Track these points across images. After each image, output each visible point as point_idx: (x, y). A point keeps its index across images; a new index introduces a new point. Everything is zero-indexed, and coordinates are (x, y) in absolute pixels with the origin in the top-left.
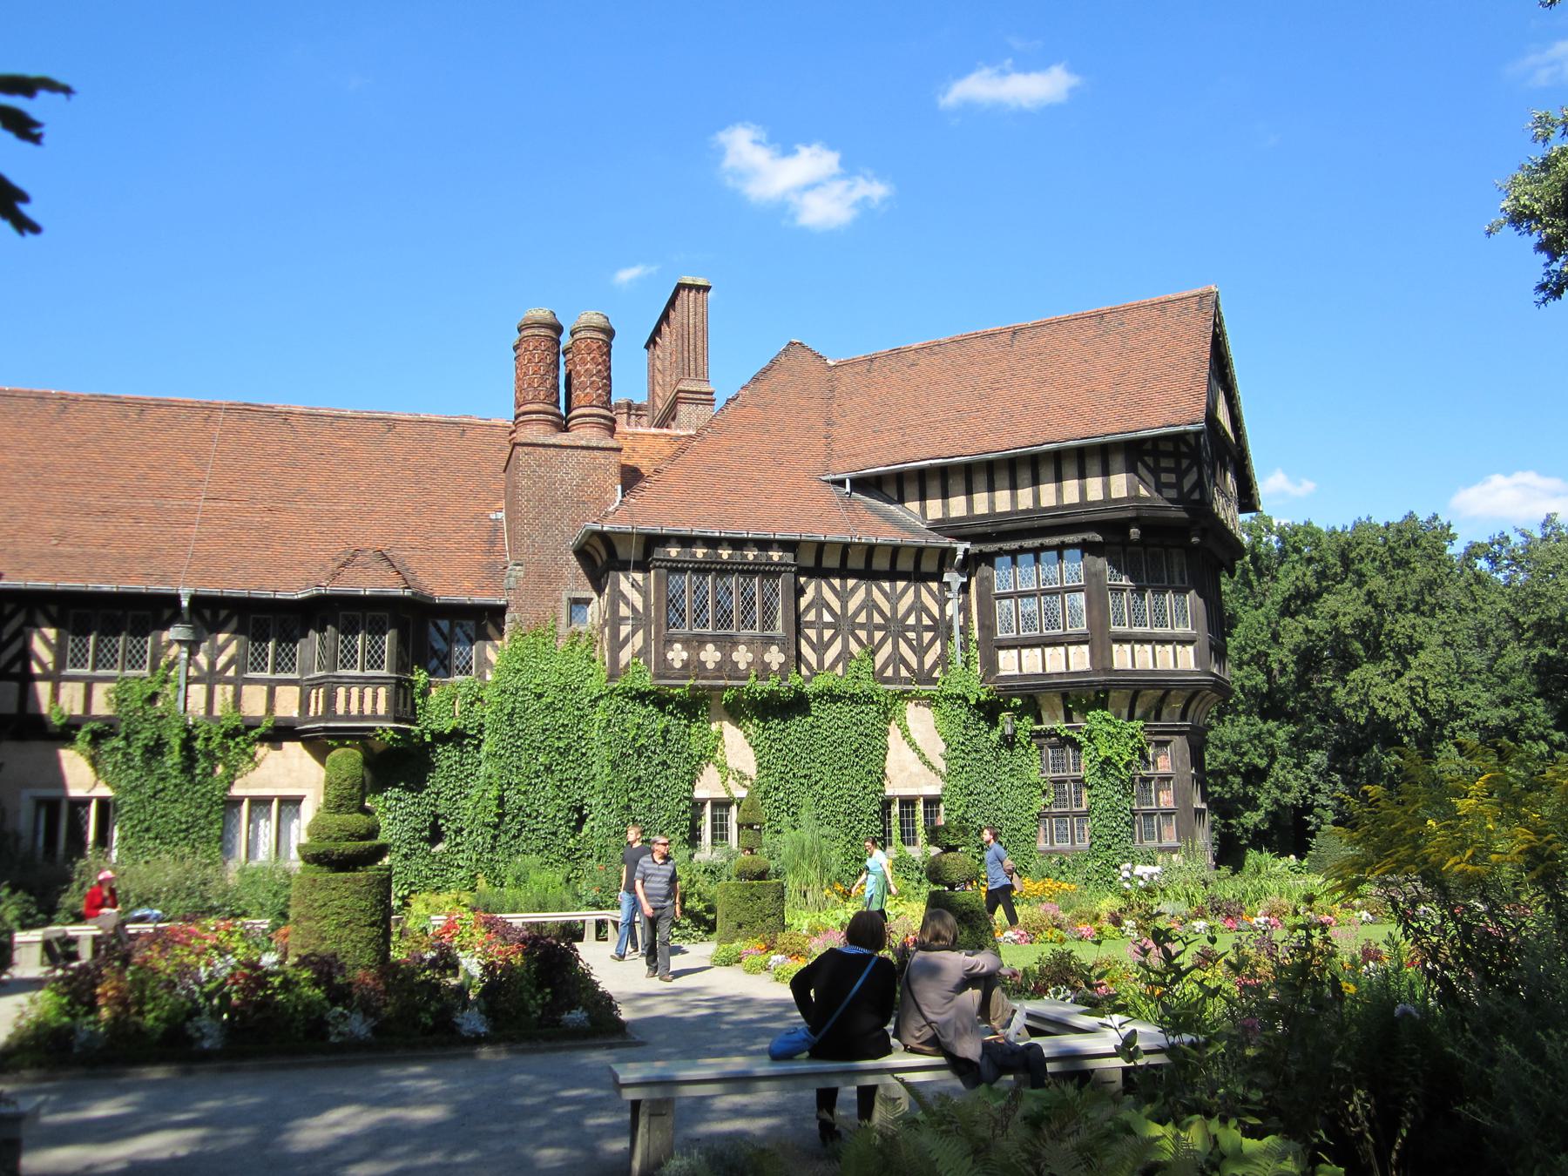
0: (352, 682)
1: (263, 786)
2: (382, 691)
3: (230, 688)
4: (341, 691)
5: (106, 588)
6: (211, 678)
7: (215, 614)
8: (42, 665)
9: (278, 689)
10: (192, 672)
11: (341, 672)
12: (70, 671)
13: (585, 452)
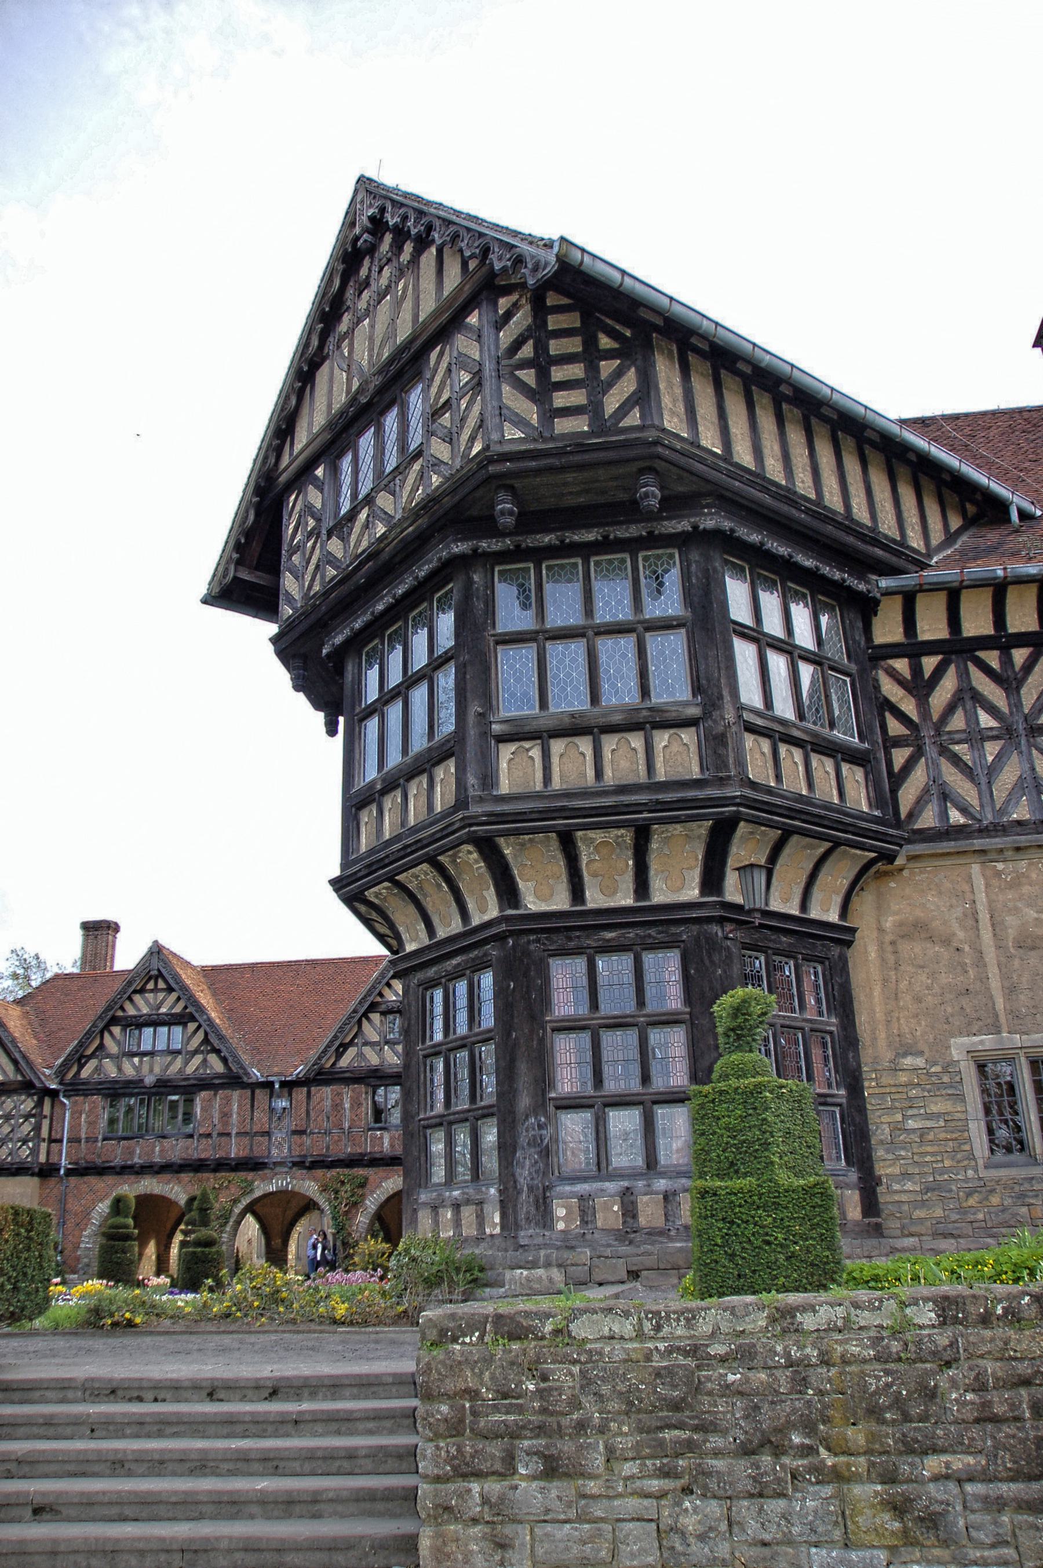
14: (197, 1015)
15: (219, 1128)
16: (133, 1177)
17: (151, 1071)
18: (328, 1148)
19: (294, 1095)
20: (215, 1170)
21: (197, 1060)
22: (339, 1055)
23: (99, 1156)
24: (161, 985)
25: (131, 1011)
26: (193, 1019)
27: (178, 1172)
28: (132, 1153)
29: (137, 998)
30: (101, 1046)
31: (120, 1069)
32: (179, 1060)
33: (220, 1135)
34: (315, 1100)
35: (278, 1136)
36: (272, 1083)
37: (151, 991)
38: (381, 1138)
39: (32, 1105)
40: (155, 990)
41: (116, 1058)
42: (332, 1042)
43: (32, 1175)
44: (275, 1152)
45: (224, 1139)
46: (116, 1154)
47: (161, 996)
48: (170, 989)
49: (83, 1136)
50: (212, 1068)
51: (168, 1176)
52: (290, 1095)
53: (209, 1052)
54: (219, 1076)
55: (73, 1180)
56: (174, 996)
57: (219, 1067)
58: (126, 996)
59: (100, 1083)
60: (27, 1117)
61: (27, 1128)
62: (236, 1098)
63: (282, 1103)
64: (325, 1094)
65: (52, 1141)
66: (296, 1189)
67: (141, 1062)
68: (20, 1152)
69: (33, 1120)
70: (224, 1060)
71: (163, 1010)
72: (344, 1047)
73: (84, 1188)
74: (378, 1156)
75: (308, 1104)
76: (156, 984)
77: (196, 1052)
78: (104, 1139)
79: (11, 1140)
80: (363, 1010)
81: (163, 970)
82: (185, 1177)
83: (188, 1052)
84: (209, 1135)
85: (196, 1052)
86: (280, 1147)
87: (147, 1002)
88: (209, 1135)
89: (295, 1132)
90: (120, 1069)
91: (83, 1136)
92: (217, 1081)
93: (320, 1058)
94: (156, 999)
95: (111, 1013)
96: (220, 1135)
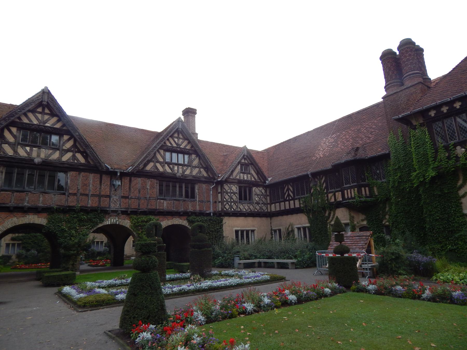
0: (347, 189)
2: (356, 189)
4: (346, 191)
5: (295, 176)
7: (320, 177)
8: (291, 197)
9: (337, 194)
11: (345, 186)
12: (296, 197)
13: (407, 90)
15: (81, 191)
17: (38, 156)
19: (123, 180)
21: (69, 155)
22: (146, 165)
24: (47, 111)
25: (25, 120)
29: (30, 115)
31: (15, 152)
33: (82, 194)
35: (114, 198)
36: (117, 172)
37: (40, 113)
38: (163, 203)
40: (43, 113)
41: (13, 146)
42: (145, 158)
44: (112, 205)
45: (84, 197)
47: (46, 117)
50: (78, 160)
53: (76, 152)
54: (82, 165)
57: (82, 160)
58: (23, 111)
62: (92, 178)
63: (118, 183)
64: (138, 182)
66: (121, 224)
67: (31, 150)
70: (86, 157)
71: (47, 125)
72: (149, 162)
74: (161, 211)
75: (130, 184)
76: (43, 109)
80: (159, 147)
81: (51, 104)
83: (63, 150)
84: (75, 194)
86: (115, 203)
87: (37, 118)
89: (123, 197)
92: (82, 168)
93: (139, 164)
94: (43, 118)
95: (12, 118)
96: (82, 194)
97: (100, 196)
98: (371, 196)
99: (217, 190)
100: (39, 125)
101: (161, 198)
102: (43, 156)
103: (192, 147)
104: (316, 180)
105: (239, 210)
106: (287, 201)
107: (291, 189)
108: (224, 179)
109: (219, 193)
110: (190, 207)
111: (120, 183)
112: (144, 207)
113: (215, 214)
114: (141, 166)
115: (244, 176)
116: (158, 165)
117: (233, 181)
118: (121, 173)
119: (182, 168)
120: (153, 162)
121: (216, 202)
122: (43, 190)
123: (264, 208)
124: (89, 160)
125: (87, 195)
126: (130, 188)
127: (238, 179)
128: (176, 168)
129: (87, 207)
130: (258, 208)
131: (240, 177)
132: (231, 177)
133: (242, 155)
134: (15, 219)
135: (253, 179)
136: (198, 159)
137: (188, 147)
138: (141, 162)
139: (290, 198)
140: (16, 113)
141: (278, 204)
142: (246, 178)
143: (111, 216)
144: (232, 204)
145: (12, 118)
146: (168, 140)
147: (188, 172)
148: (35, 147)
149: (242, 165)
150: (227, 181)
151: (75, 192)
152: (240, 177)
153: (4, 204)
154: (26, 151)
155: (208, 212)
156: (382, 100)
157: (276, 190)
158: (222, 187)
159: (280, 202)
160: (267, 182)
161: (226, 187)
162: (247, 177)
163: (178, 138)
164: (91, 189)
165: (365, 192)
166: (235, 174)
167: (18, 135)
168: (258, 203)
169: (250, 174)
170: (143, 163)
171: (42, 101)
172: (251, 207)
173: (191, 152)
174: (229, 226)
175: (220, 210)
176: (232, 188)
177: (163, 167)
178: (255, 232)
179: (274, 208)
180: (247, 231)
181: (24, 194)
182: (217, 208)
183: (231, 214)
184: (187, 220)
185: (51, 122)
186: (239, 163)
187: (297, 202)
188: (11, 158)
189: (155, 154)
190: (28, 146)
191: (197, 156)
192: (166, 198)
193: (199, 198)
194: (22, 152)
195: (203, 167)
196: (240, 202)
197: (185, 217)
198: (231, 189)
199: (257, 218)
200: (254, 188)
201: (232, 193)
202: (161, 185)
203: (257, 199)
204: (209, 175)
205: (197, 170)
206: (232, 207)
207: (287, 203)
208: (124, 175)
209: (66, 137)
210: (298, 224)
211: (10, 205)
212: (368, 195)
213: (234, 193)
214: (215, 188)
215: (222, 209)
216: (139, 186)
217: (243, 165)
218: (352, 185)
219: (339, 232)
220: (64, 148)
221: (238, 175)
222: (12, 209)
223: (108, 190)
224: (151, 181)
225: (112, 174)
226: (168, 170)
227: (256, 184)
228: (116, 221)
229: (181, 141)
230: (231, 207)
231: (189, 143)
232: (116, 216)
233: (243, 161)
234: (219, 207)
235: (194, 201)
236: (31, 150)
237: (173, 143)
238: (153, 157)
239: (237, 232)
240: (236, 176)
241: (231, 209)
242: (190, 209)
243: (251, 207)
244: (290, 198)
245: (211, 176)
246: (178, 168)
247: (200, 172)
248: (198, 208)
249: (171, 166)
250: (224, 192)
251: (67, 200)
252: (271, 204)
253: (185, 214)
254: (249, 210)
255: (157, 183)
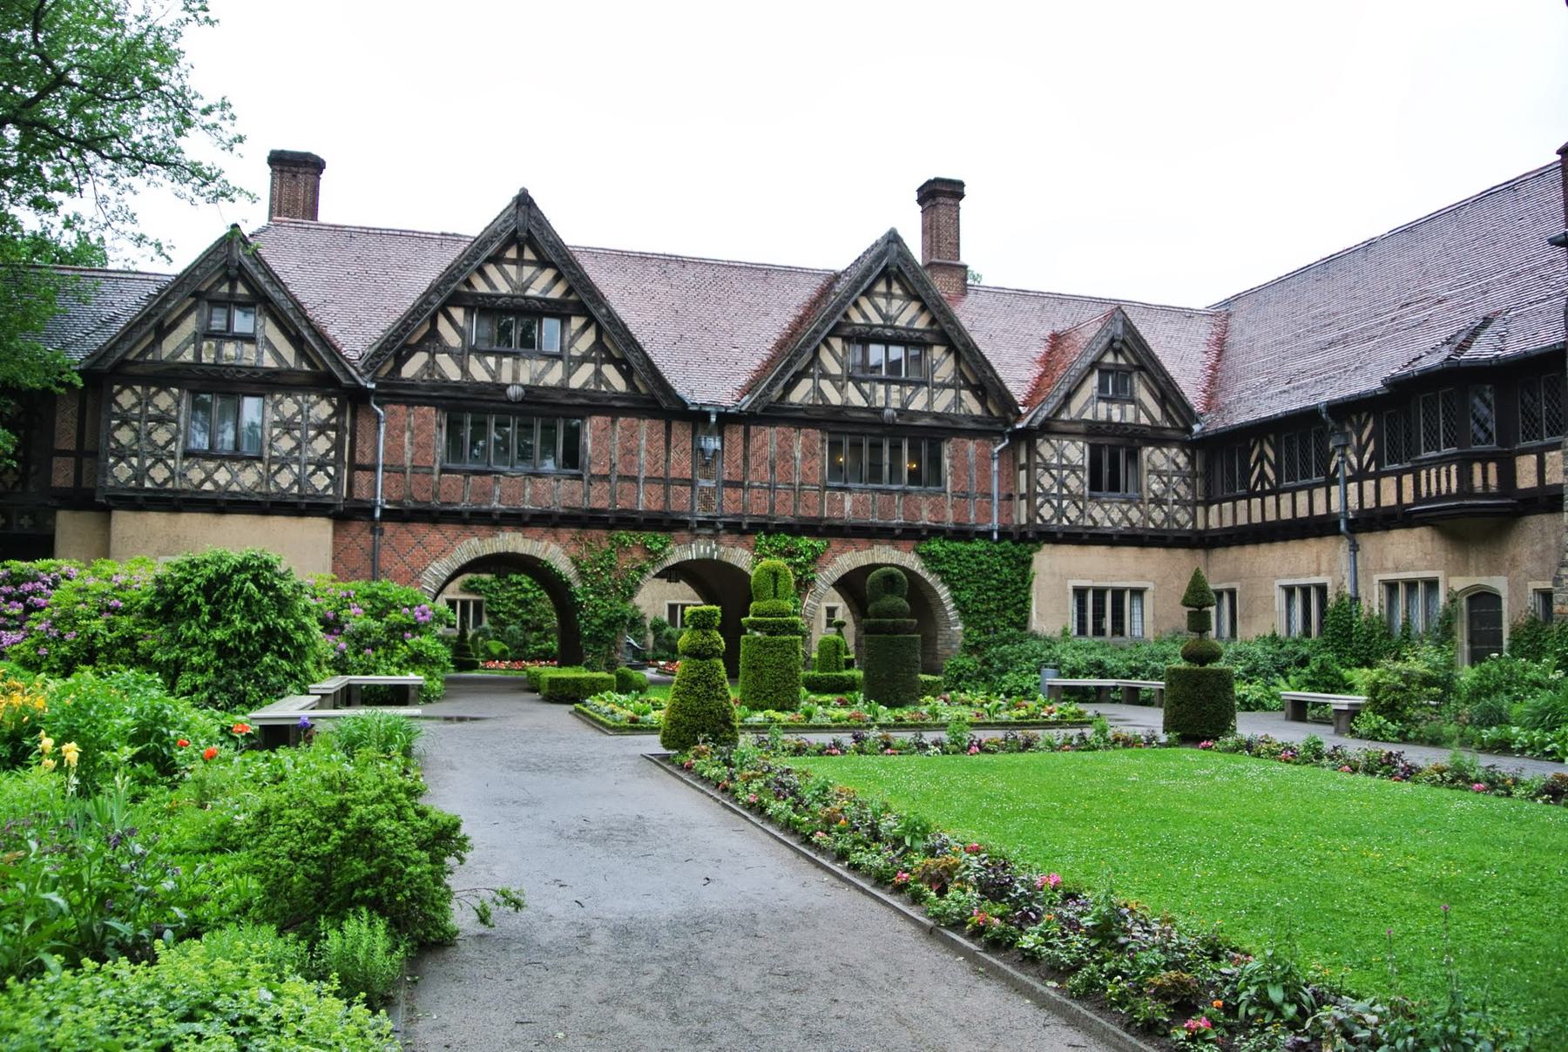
1: (1407, 570)
2: (1454, 468)
3: (1373, 482)
4: (1423, 473)
6: (1360, 476)
7: (1359, 418)
10: (1349, 473)
11: (1424, 455)
14: (591, 306)
15: (620, 468)
16: (484, 530)
18: (772, 508)
19: (727, 434)
20: (611, 527)
21: (587, 370)
22: (789, 387)
23: (436, 495)
24: (529, 255)
25: (481, 287)
26: (581, 309)
27: (555, 526)
28: (488, 494)
29: (491, 270)
30: (433, 334)
31: (465, 371)
32: (559, 365)
33: (622, 478)
34: (755, 444)
36: (708, 414)
38: (842, 501)
39: (330, 410)
40: (519, 262)
41: (460, 357)
43: (329, 516)
45: (627, 485)
46: (461, 492)
47: (528, 271)
48: (543, 263)
49: (408, 464)
50: (608, 384)
51: (540, 530)
52: (721, 434)
53: (603, 362)
54: (618, 396)
55: (389, 527)
56: (549, 274)
57: (619, 384)
58: (476, 264)
59: (434, 389)
60: (322, 429)
61: (322, 445)
62: (646, 432)
63: (713, 443)
64: (768, 439)
65: (354, 467)
66: (724, 558)
67: (499, 364)
68: (314, 480)
69: (333, 434)
70: (627, 375)
71: (531, 292)
73: (409, 539)
75: (746, 448)
76: (520, 252)
77: (584, 359)
78: (443, 471)
79: (297, 460)
82: (566, 534)
84: (605, 478)
85: (584, 359)
88: (605, 478)
90: (465, 371)
91: (408, 464)
92: (618, 404)
94: (520, 274)
96: (622, 478)
97: (666, 482)
98: (1461, 494)
99: (1016, 458)
100: (513, 297)
101: (836, 484)
102: (525, 378)
103: (933, 321)
104: (1348, 429)
105: (1090, 523)
106: (1257, 495)
107: (1271, 455)
108: (1036, 424)
109: (1022, 468)
110: (925, 513)
111: (718, 445)
112: (786, 512)
113: (1004, 534)
114: (776, 393)
115: (1109, 411)
116: (826, 386)
117: (1072, 428)
118: (719, 415)
119: (900, 391)
120: (812, 376)
121: (1010, 497)
122: (530, 469)
123: (1183, 517)
124: (637, 383)
125: (634, 479)
126: (746, 458)
127: (1086, 421)
128: (881, 389)
129: (638, 512)
130: (1158, 515)
131: (1095, 414)
132: (1064, 416)
133: (1106, 340)
134: (475, 541)
135: (1144, 420)
136: (952, 357)
137: (922, 323)
138: (776, 379)
139: (1267, 487)
140: (461, 272)
141: (1228, 505)
142: (1116, 418)
143: (698, 536)
144: (1065, 503)
145: (453, 286)
146: (856, 304)
147: (918, 404)
148: (506, 354)
149: (1104, 373)
150: (1047, 429)
151: (606, 470)
152: (1095, 414)
153: (449, 503)
154: (487, 368)
155: (982, 528)
156: (1559, 157)
157: (1224, 456)
158: (1032, 450)
159: (1234, 500)
160: (1196, 428)
161: (1045, 449)
162: (1123, 414)
163: (889, 296)
164: (644, 463)
165: (1485, 478)
166: (1076, 404)
167: (467, 327)
168: (1159, 501)
169: (1133, 401)
170: (782, 383)
171: (515, 231)
172: (1134, 514)
173: (928, 338)
174: (1054, 574)
175: (1024, 521)
176: (1067, 452)
177: (840, 390)
178: (1147, 597)
179: (1217, 517)
180: (1118, 594)
181: (489, 479)
182: (1015, 516)
183: (1060, 536)
184: (916, 551)
185: (542, 285)
186: (1094, 365)
187: (1388, 484)
188: (457, 386)
189: (816, 351)
190: (491, 353)
191: (948, 352)
192: (850, 485)
193: (955, 484)
194: (479, 372)
195: (968, 386)
196: (1091, 498)
197: (911, 544)
198: (1062, 456)
199: (1155, 550)
200: (1146, 451)
201: (1064, 467)
202: (835, 447)
203: (1155, 487)
204: (989, 411)
205: (950, 393)
206: (1064, 514)
207: (1256, 502)
208: (727, 419)
209: (576, 323)
210: (1289, 576)
211: (461, 506)
212: (1493, 489)
213: (1073, 469)
214: (1010, 453)
215: (1028, 519)
216: (771, 449)
217: (1109, 372)
218: (1444, 451)
219: (1200, 608)
220: (574, 352)
221: (1088, 405)
222: (467, 516)
223: (687, 463)
224: (806, 436)
225: (697, 418)
226: (857, 399)
227: (1157, 438)
228: (712, 551)
229: (897, 303)
230: (1060, 512)
231: (923, 308)
232: (711, 537)
233: (1109, 359)
234: (1021, 515)
235: (938, 494)
236: (499, 364)
237: (868, 313)
238: (811, 363)
239: (1080, 593)
240: (1082, 411)
241: (1060, 520)
242: (926, 518)
243: (1134, 514)
244: (1267, 487)
245: (995, 412)
246: (887, 391)
247: (958, 401)
248: (949, 518)
249: (866, 387)
250: (1037, 465)
251: (587, 494)
252: (1207, 504)
253: (910, 534)
254: (1126, 524)
255: (823, 441)
